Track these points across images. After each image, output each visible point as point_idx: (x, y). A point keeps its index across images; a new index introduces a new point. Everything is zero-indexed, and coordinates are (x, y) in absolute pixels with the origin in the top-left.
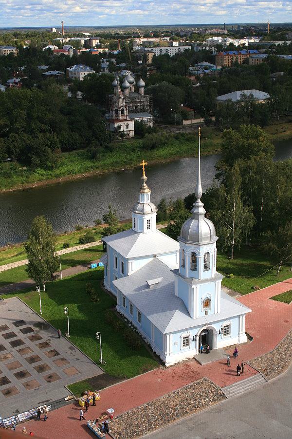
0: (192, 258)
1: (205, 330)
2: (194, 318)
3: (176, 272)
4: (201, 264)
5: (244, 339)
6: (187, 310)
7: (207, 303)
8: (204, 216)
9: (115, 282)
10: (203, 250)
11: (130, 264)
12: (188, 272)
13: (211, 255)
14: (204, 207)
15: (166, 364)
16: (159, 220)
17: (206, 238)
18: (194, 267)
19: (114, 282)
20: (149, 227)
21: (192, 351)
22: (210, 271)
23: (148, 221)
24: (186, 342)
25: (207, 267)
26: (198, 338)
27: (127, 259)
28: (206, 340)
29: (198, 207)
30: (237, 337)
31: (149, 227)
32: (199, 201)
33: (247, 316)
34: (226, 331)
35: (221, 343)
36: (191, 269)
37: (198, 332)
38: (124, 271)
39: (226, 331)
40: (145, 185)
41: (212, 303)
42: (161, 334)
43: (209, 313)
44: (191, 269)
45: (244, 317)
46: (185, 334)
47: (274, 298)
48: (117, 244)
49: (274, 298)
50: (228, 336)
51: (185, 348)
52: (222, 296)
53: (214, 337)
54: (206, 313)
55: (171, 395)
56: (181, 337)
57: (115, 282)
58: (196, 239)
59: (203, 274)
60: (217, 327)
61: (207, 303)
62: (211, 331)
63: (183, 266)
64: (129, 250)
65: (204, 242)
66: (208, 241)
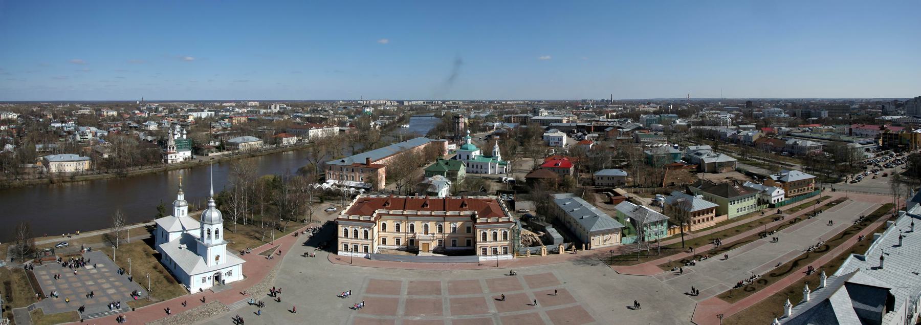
1: (217, 273)
5: (242, 278)
7: (217, 258)
9: (161, 246)
14: (216, 203)
16: (190, 211)
17: (216, 220)
18: (209, 237)
19: (160, 245)
20: (183, 214)
21: (209, 285)
24: (204, 280)
26: (212, 277)
27: (169, 233)
29: (211, 202)
30: (237, 276)
31: (183, 214)
33: (243, 264)
34: (230, 273)
37: (212, 274)
38: (167, 240)
39: (230, 273)
40: (181, 189)
41: (220, 258)
42: (188, 275)
45: (241, 265)
46: (203, 275)
47: (261, 254)
48: (162, 222)
49: (261, 254)
51: (203, 284)
52: (227, 254)
54: (217, 263)
55: (193, 309)
57: (161, 246)
59: (214, 240)
60: (224, 272)
61: (217, 258)
64: (170, 227)
66: (218, 222)
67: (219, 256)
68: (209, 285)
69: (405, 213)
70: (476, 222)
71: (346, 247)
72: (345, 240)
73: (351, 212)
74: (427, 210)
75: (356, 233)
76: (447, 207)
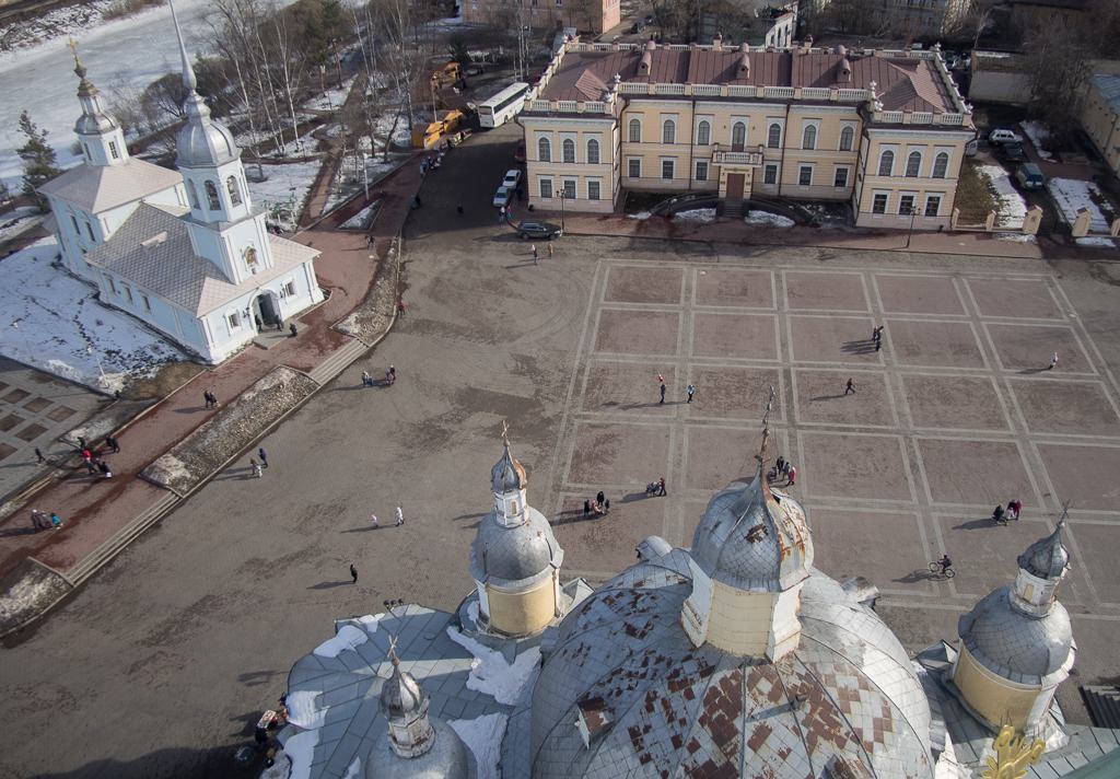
0: (209, 192)
1: (260, 297)
2: (238, 283)
3: (187, 217)
4: (226, 198)
6: (224, 276)
7: (251, 255)
8: (208, 117)
10: (224, 173)
11: (103, 223)
12: (206, 215)
13: (237, 179)
15: (214, 363)
21: (248, 332)
22: (243, 205)
23: (112, 145)
24: (234, 320)
25: (236, 200)
28: (266, 313)
29: (195, 103)
31: (115, 155)
32: (195, 93)
33: (315, 259)
35: (287, 310)
36: (211, 209)
41: (258, 255)
43: (257, 271)
44: (211, 209)
50: (293, 297)
53: (275, 306)
56: (224, 317)
58: (206, 160)
59: (234, 212)
61: (251, 255)
62: (269, 295)
63: (197, 206)
65: (221, 160)
67: (252, 251)
68: (248, 332)
69: (689, 90)
70: (870, 120)
71: (546, 185)
72: (545, 167)
73: (549, 94)
74: (746, 82)
75: (569, 147)
76: (794, 79)
